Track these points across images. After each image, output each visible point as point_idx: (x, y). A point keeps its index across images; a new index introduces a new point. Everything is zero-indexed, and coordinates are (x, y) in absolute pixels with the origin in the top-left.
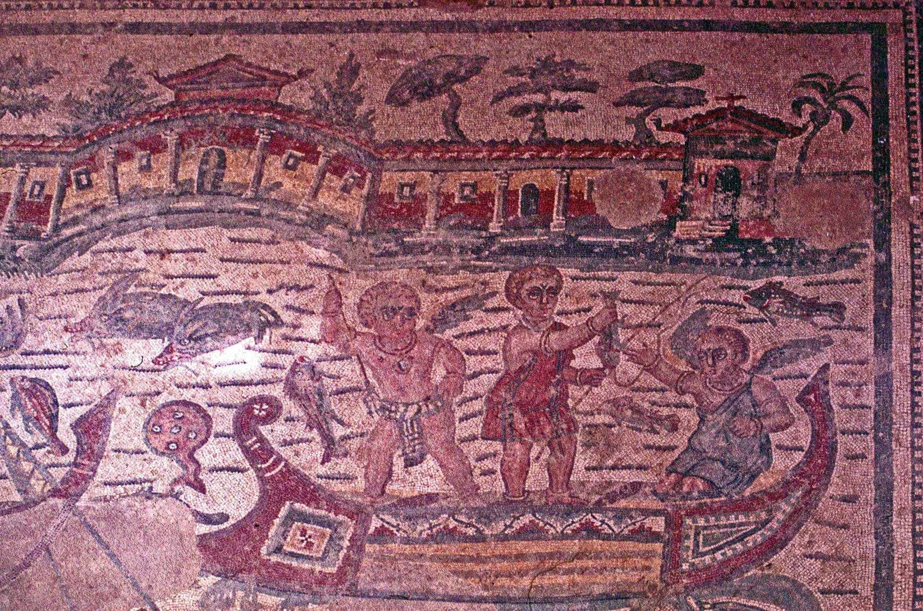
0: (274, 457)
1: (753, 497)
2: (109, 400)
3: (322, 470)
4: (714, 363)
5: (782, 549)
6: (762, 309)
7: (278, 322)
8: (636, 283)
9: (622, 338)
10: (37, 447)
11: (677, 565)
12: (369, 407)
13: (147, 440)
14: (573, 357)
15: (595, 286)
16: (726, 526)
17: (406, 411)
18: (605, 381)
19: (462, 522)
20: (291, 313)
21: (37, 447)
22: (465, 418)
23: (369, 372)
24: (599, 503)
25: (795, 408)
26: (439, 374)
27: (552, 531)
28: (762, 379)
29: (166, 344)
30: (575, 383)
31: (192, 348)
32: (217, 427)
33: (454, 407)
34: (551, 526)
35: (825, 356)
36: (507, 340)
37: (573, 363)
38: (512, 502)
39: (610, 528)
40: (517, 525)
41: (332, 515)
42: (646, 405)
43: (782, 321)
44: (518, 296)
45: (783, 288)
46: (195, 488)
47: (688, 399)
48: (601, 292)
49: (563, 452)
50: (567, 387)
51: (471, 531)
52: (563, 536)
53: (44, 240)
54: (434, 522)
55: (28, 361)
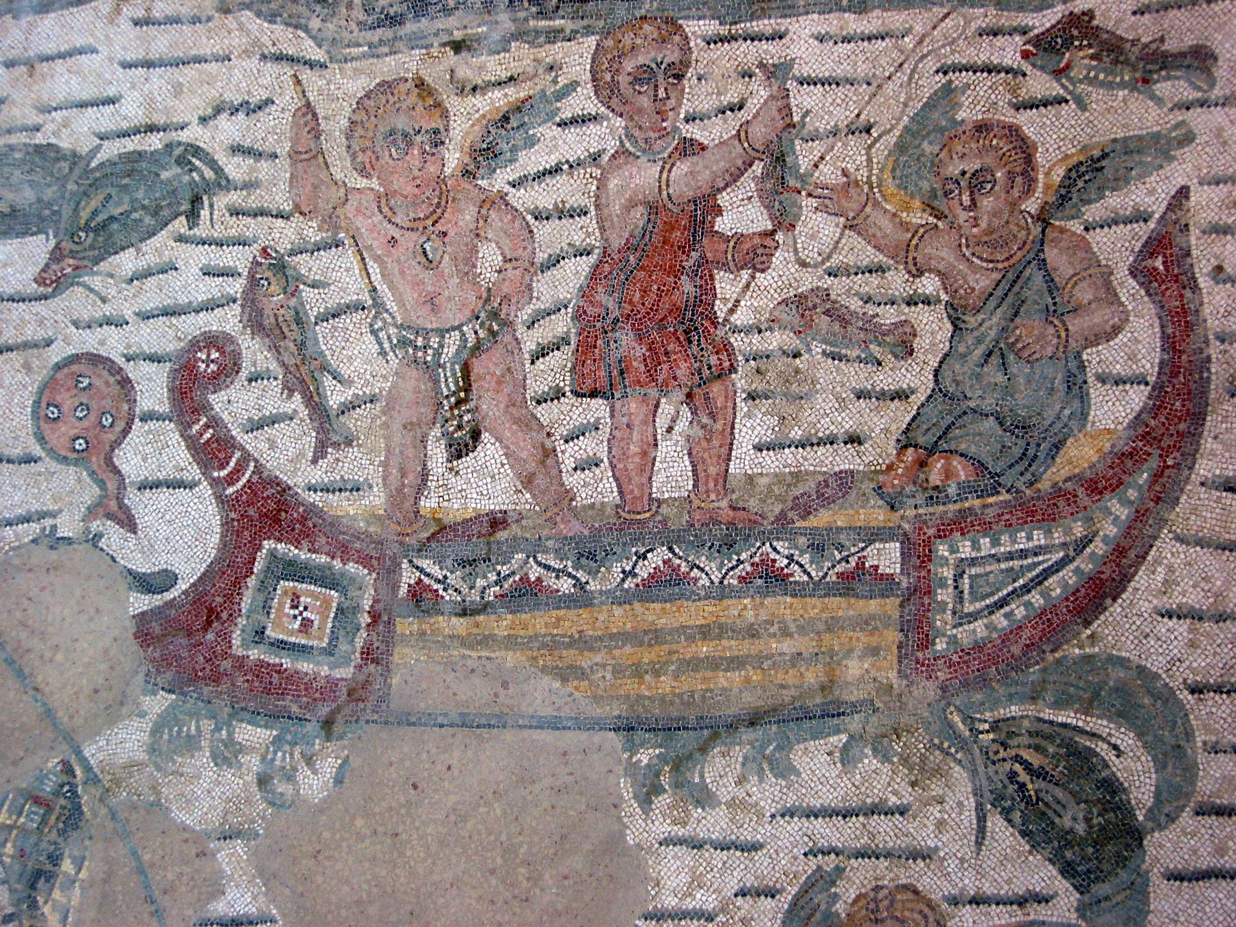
0: (238, 454)
1: (1058, 492)
3: (317, 475)
4: (973, 200)
5: (1114, 600)
6: (1058, 73)
7: (223, 183)
8: (821, 39)
9: (804, 164)
11: (926, 643)
12: (380, 344)
13: (41, 439)
14: (719, 211)
15: (747, 53)
16: (1010, 556)
17: (441, 346)
18: (778, 258)
19: (547, 567)
20: (238, 159)
22: (542, 352)
23: (374, 268)
24: (782, 517)
25: (1128, 289)
26: (489, 256)
27: (704, 581)
28: (1062, 230)
29: (52, 243)
30: (724, 266)
31: (92, 247)
33: (521, 331)
34: (702, 570)
35: (1179, 172)
36: (602, 183)
37: (723, 224)
38: (632, 522)
39: (805, 571)
40: (643, 571)
41: (337, 564)
42: (855, 304)
43: (1096, 96)
44: (614, 86)
45: (1095, 23)
46: (120, 523)
47: (929, 285)
48: (761, 65)
49: (712, 416)
50: (712, 277)
51: (565, 585)
52: (721, 592)
54: (505, 570)
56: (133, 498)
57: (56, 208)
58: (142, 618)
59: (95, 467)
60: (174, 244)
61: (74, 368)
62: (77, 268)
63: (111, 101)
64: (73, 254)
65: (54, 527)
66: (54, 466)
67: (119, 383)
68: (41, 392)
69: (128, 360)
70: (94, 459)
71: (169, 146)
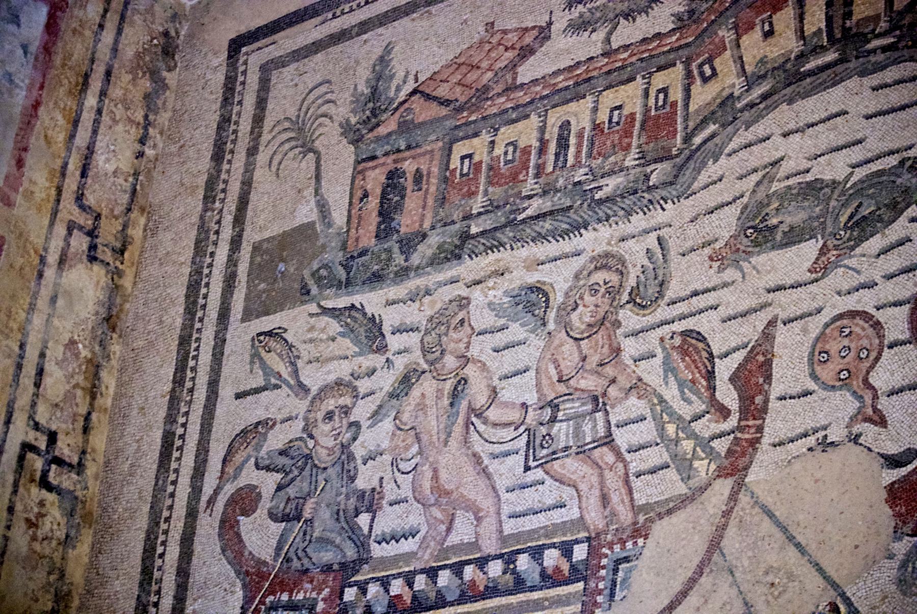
2: (767, 336)
10: (697, 418)
13: (814, 377)
21: (697, 418)
29: (821, 242)
31: (849, 240)
32: (890, 337)
46: (875, 423)
53: (677, 156)
55: (681, 308)
56: (884, 403)
57: (822, 220)
58: (891, 488)
59: (855, 388)
60: (908, 225)
61: (838, 323)
62: (839, 255)
63: (860, 142)
64: (836, 247)
65: (826, 437)
66: (823, 393)
67: (872, 326)
68: (814, 347)
69: (878, 309)
70: (855, 383)
71: (902, 163)
